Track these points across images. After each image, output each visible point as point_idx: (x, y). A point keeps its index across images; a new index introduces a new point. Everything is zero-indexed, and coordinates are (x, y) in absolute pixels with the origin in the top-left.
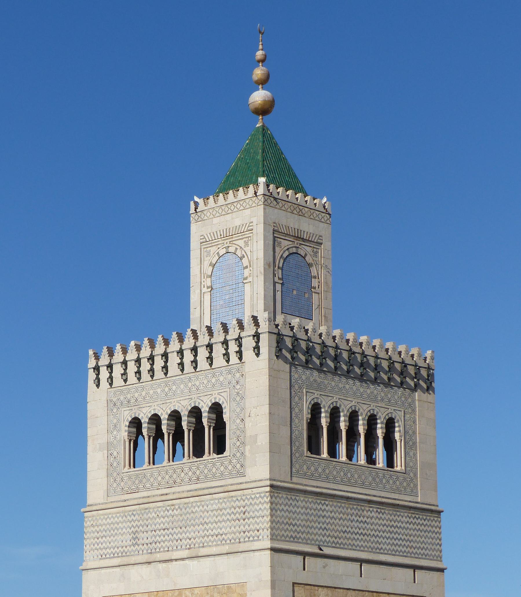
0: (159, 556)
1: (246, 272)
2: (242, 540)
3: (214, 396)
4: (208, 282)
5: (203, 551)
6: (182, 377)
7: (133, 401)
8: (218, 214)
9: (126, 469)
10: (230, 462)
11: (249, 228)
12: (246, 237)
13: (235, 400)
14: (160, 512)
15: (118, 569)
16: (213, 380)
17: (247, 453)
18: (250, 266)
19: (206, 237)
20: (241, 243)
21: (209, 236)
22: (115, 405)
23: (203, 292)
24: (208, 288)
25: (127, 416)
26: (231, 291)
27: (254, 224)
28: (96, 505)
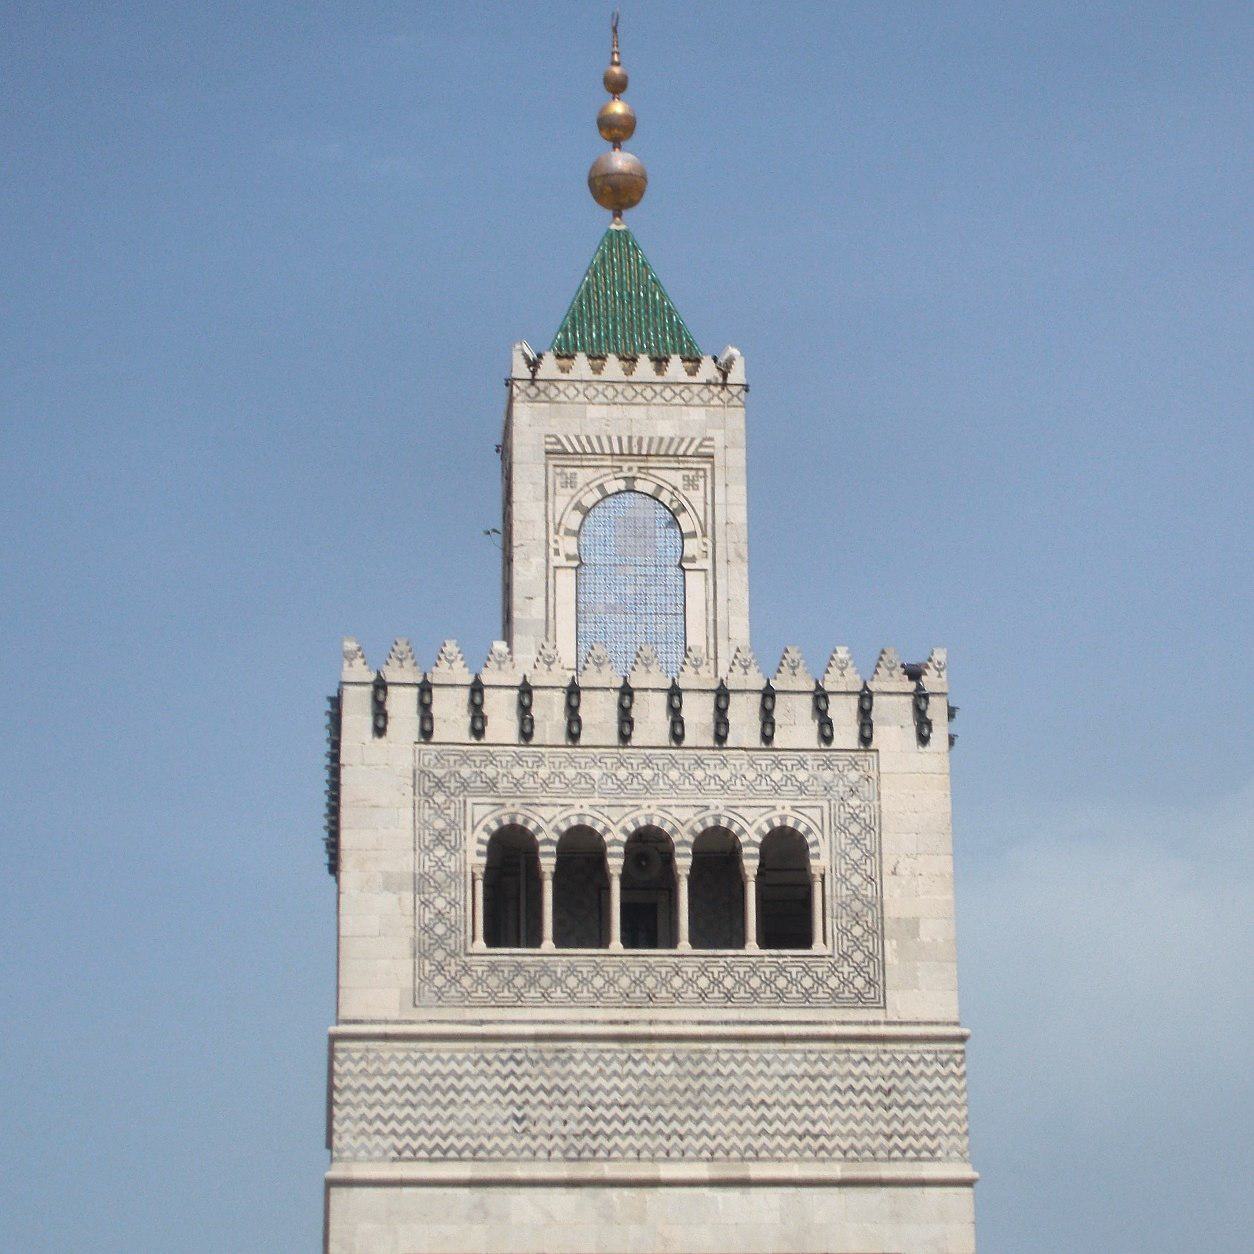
0: (608, 1171)
1: (692, 547)
2: (882, 1154)
3: (780, 812)
4: (569, 545)
5: (756, 1171)
7: (503, 784)
9: (480, 945)
10: (834, 970)
11: (702, 450)
13: (844, 829)
14: (608, 1063)
15: (465, 1192)
16: (777, 775)
17: (891, 958)
19: (564, 441)
21: (575, 442)
23: (552, 564)
24: (569, 557)
25: (482, 819)
27: (719, 442)
28: (373, 1022)
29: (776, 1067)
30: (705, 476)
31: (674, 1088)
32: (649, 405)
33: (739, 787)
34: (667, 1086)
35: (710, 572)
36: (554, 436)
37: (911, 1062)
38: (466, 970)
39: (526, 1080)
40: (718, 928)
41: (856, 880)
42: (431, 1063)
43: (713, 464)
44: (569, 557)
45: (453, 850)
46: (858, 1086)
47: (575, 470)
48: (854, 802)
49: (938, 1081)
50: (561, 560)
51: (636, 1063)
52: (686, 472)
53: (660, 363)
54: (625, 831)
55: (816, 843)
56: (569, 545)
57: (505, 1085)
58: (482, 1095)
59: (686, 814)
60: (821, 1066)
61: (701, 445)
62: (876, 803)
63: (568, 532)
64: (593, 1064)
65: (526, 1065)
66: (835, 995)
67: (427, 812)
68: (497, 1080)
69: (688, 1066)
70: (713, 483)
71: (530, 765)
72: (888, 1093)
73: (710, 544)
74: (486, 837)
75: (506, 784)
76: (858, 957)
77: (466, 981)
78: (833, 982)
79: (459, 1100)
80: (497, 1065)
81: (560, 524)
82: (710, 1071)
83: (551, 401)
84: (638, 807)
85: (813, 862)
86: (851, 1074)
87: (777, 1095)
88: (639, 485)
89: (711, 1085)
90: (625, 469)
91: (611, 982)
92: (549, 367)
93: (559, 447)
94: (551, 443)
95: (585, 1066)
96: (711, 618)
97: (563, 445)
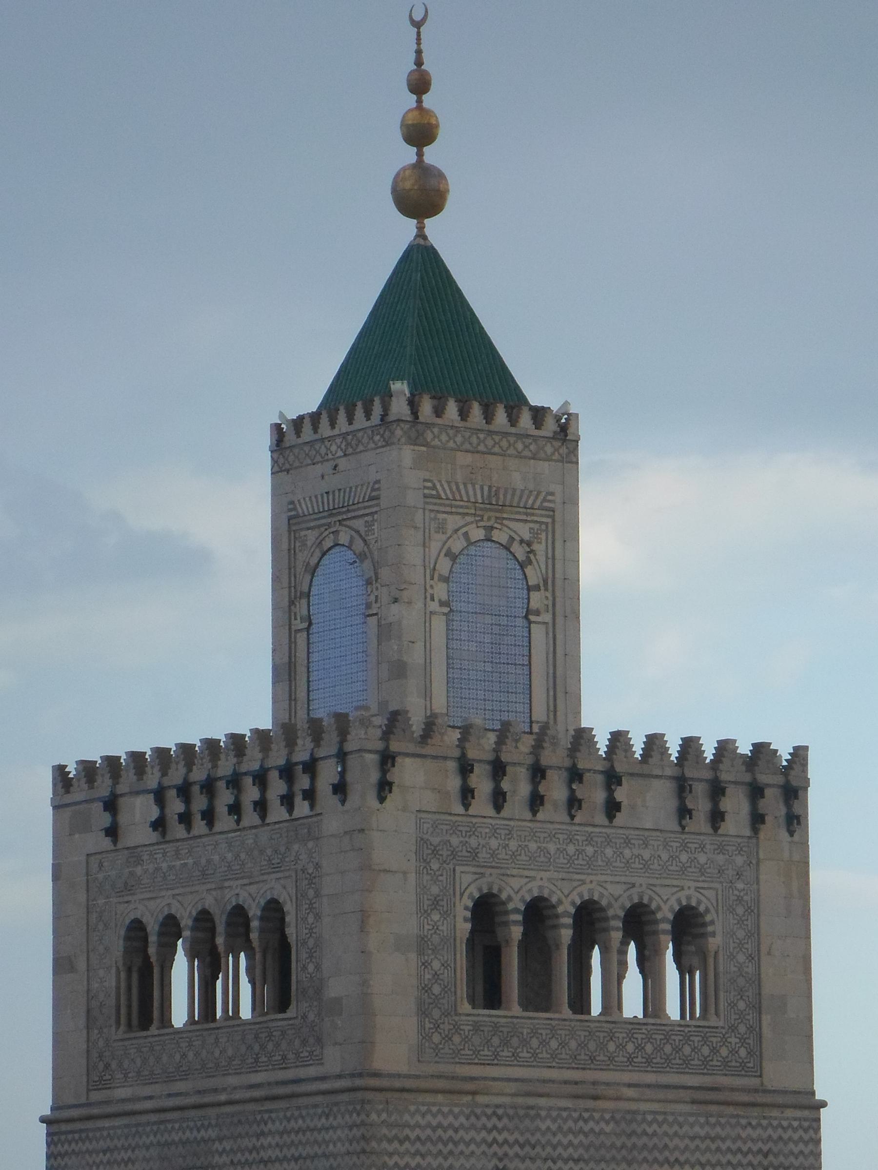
1: (537, 599)
3: (687, 892)
4: (440, 591)
6: (609, 831)
7: (483, 855)
8: (467, 446)
9: (466, 1007)
11: (546, 504)
12: (536, 522)
14: (565, 1120)
16: (684, 857)
17: (766, 1031)
19: (438, 487)
20: (524, 531)
22: (435, 852)
25: (469, 886)
26: (496, 629)
27: (558, 498)
29: (686, 1128)
30: (547, 530)
31: (613, 1146)
32: (505, 455)
33: (656, 866)
34: (608, 1143)
35: (551, 625)
37: (783, 1128)
38: (457, 1028)
39: (505, 1135)
41: (741, 958)
42: (434, 1116)
43: (553, 517)
44: (442, 604)
45: (445, 915)
46: (745, 1149)
47: (445, 516)
48: (740, 886)
49: (801, 1146)
51: (586, 1121)
52: (532, 525)
54: (573, 903)
55: (712, 922)
56: (440, 591)
57: (490, 1139)
58: (473, 1147)
59: (617, 890)
60: (718, 1129)
61: (545, 500)
62: (755, 886)
64: (554, 1120)
65: (505, 1120)
66: (725, 1063)
67: (426, 878)
68: (484, 1134)
69: (623, 1125)
70: (553, 536)
71: (503, 837)
72: (766, 1156)
73: (551, 598)
74: (470, 904)
75: (485, 855)
76: (742, 1029)
77: (457, 1039)
78: (724, 1052)
79: (457, 1151)
80: (484, 1119)
81: (434, 569)
82: (639, 1131)
83: (427, 445)
84: (583, 882)
85: (711, 940)
86: (739, 1137)
87: (687, 1155)
88: (496, 535)
89: (640, 1143)
90: (485, 518)
91: (563, 1045)
92: (426, 407)
93: (434, 492)
94: (428, 488)
95: (548, 1123)
96: (551, 671)
97: (437, 492)
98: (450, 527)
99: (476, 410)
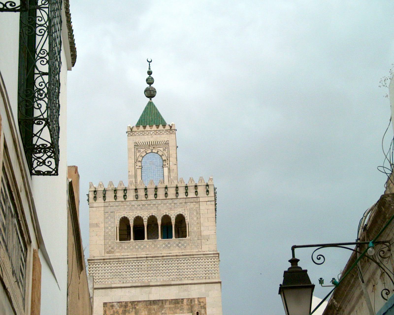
11: (166, 143)
18: (168, 160)
36: (136, 142)
40: (167, 234)
43: (169, 146)
44: (139, 166)
47: (140, 149)
50: (138, 167)
53: (158, 126)
55: (187, 217)
56: (139, 164)
61: (166, 142)
63: (139, 161)
73: (169, 162)
85: (186, 221)
88: (154, 151)
90: (151, 148)
98: (142, 151)
99: (148, 126)
